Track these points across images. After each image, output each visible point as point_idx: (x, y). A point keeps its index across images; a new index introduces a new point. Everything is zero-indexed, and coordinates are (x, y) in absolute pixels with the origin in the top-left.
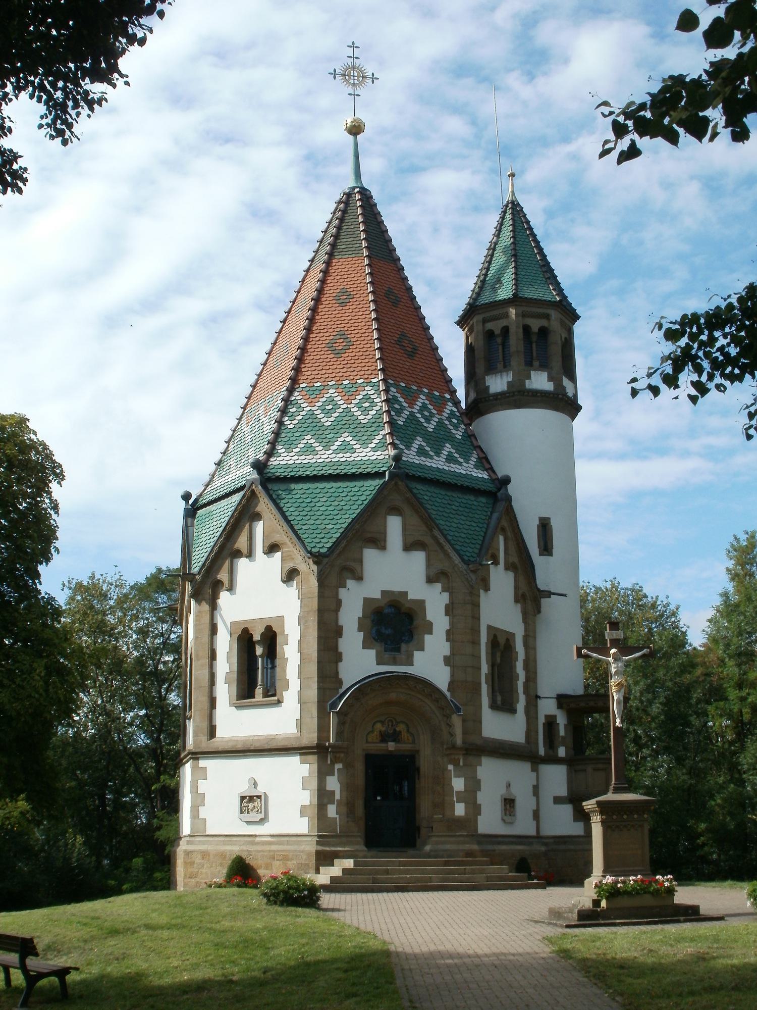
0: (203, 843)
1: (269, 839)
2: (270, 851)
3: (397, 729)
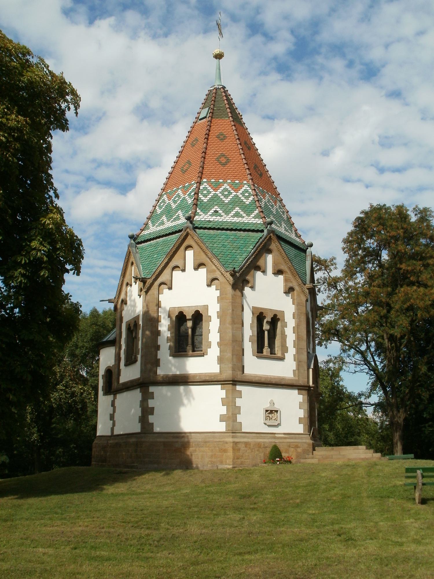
0: (244, 437)
1: (283, 436)
2: (288, 442)
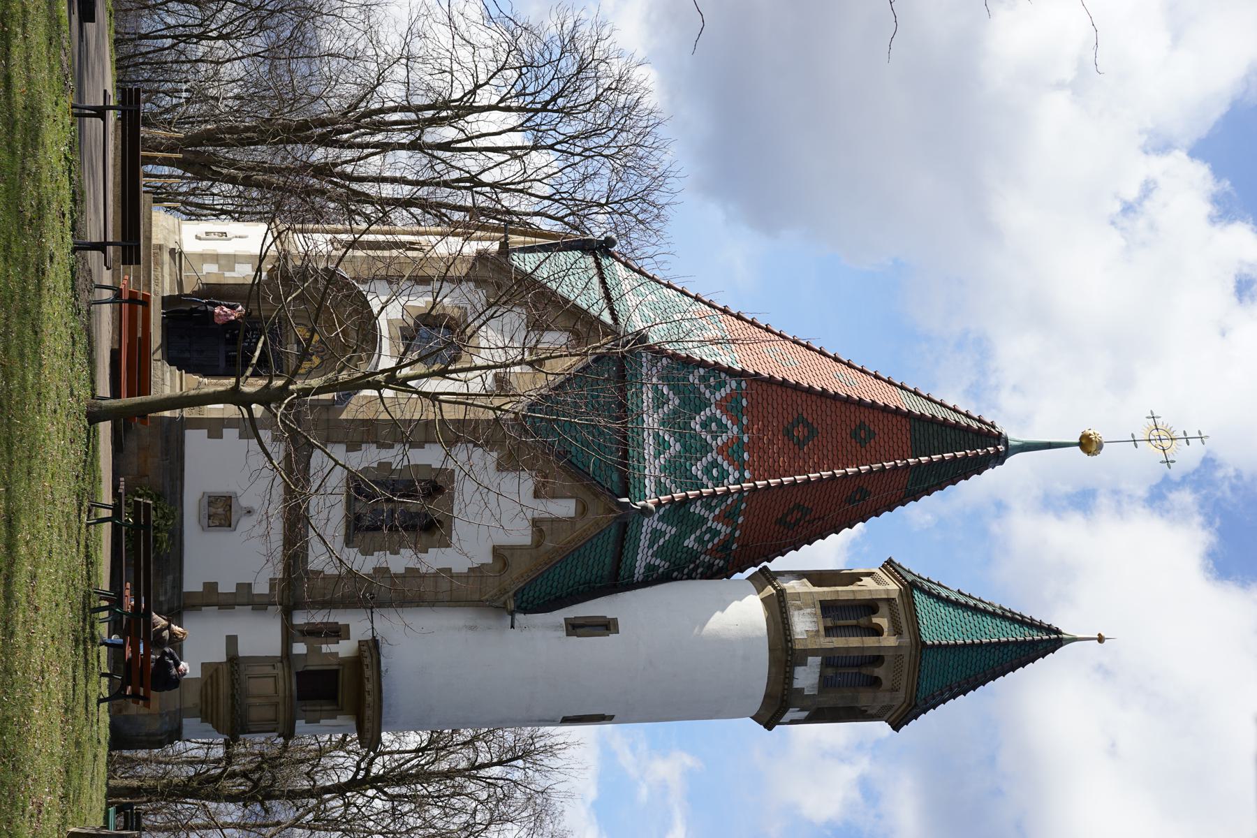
3: (314, 357)
